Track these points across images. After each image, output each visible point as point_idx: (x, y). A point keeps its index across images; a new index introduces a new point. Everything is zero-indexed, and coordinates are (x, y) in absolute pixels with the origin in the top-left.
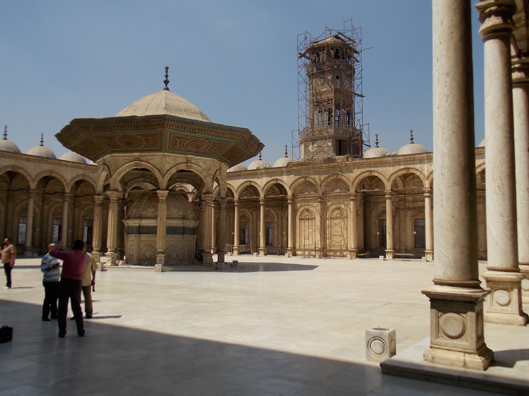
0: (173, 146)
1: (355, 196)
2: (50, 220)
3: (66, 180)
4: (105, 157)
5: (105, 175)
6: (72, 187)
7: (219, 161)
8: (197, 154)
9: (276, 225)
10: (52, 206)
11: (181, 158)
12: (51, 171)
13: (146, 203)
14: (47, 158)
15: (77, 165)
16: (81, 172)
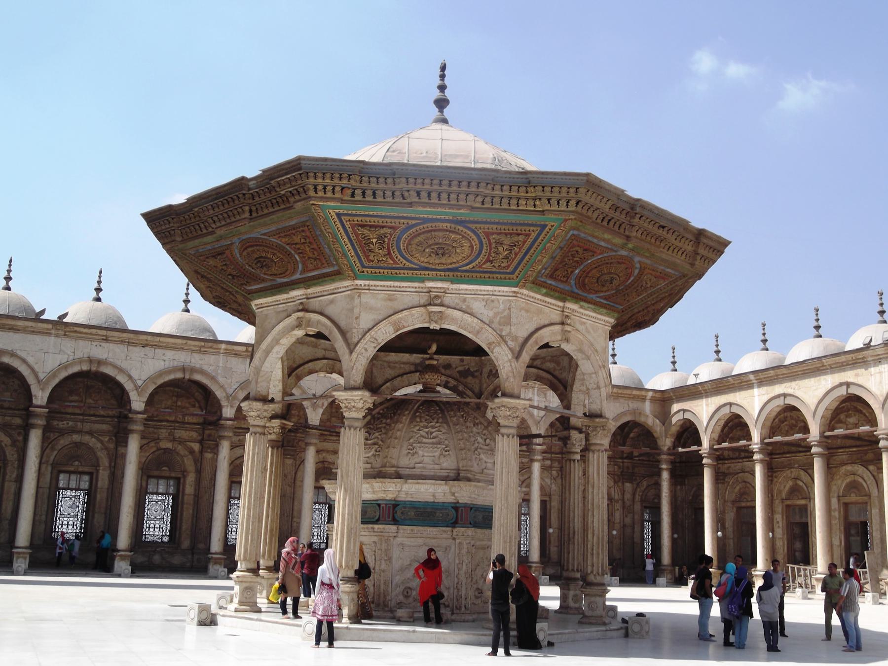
0: (367, 257)
8: (455, 274)
11: (409, 291)
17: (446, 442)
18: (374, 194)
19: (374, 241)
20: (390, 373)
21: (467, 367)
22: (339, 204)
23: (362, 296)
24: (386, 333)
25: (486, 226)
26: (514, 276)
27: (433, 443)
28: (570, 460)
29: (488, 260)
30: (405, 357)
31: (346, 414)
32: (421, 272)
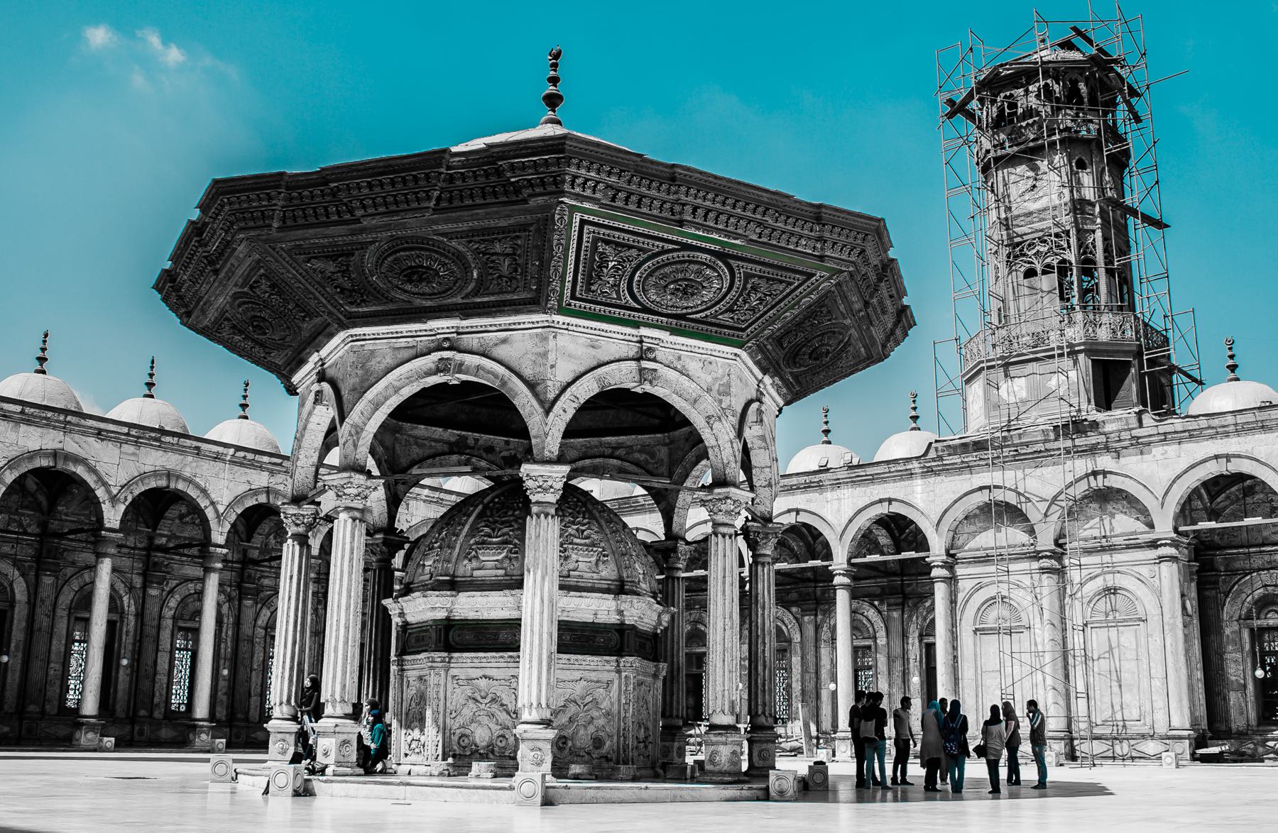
0: (589, 283)
1: (1175, 544)
2: (165, 635)
3: (213, 503)
4: (324, 352)
5: (325, 428)
6: (234, 526)
7: (757, 363)
8: (682, 324)
9: (882, 660)
10: (171, 591)
11: (616, 340)
12: (169, 475)
13: (474, 531)
14: (162, 431)
15: (250, 456)
16: (261, 479)
17: (602, 544)
18: (639, 203)
19: (611, 265)
20: (416, 452)
21: (513, 452)
22: (596, 208)
23: (559, 337)
24: (587, 389)
25: (750, 266)
26: (744, 334)
27: (585, 545)
28: (673, 578)
29: (730, 310)
30: (438, 432)
31: (533, 498)
32: (636, 313)
